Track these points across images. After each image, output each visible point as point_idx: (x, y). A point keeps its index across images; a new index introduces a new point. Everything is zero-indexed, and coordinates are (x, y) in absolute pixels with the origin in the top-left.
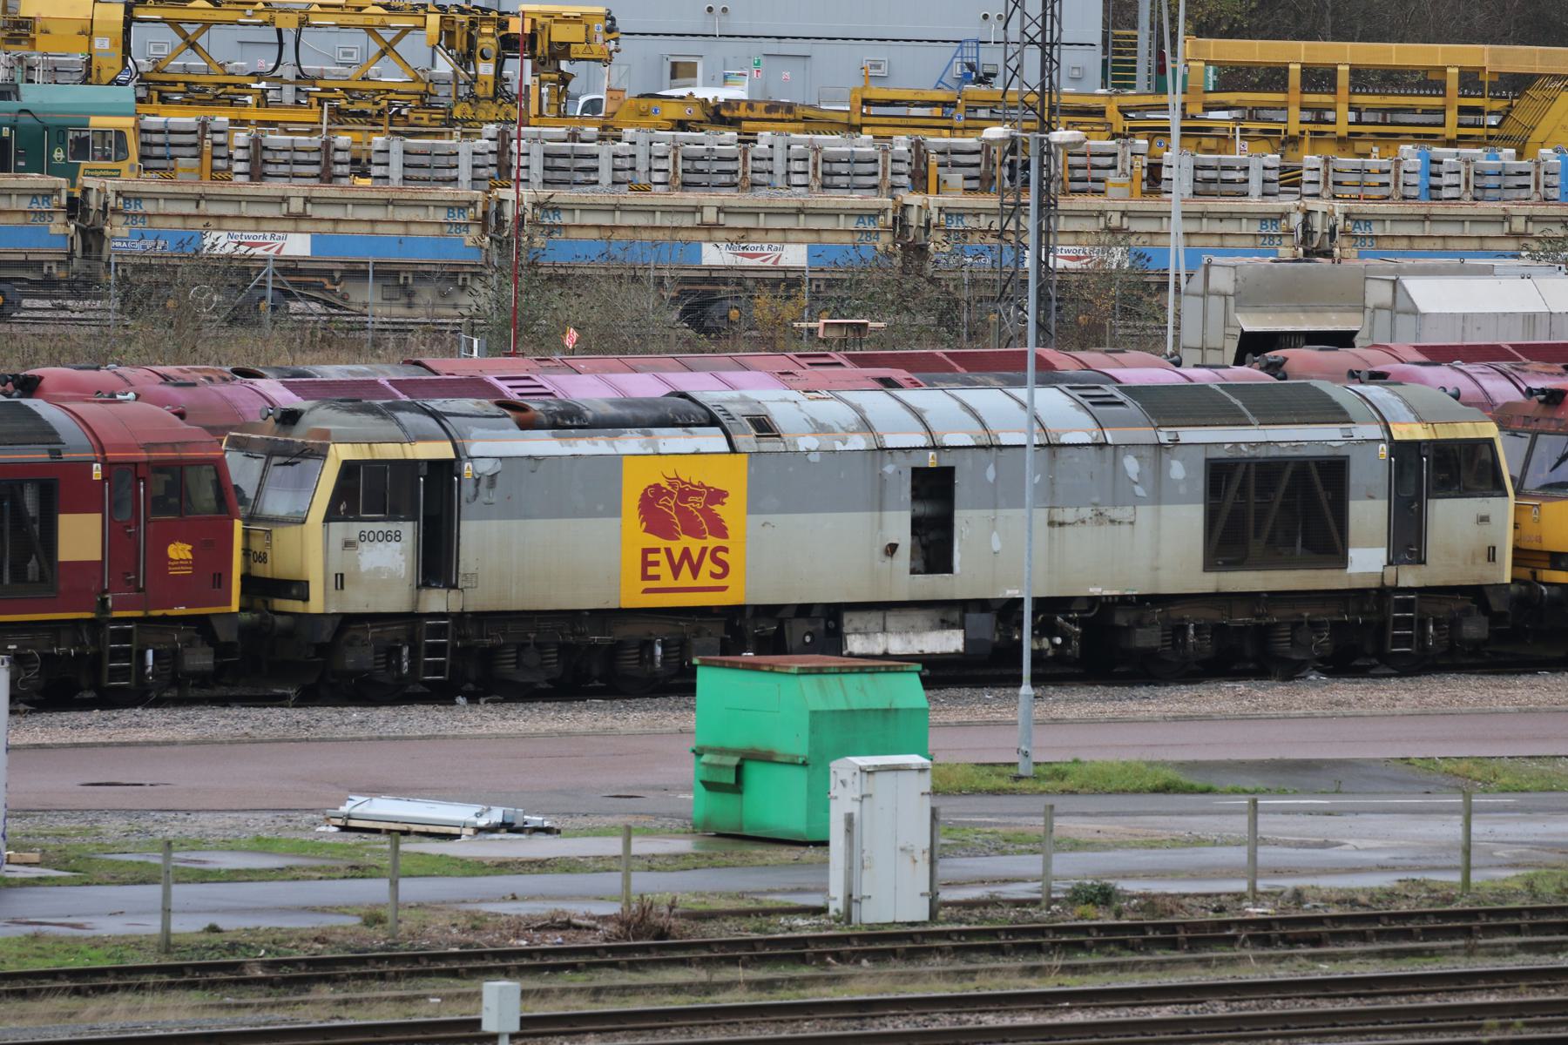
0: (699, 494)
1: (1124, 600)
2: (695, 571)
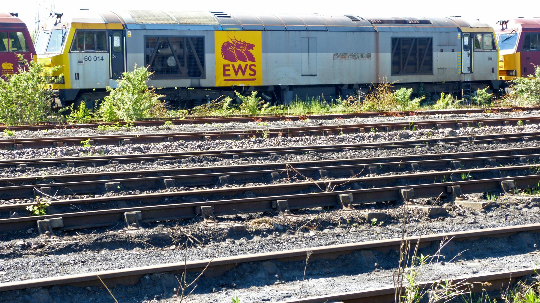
0: (244, 46)
2: (244, 73)
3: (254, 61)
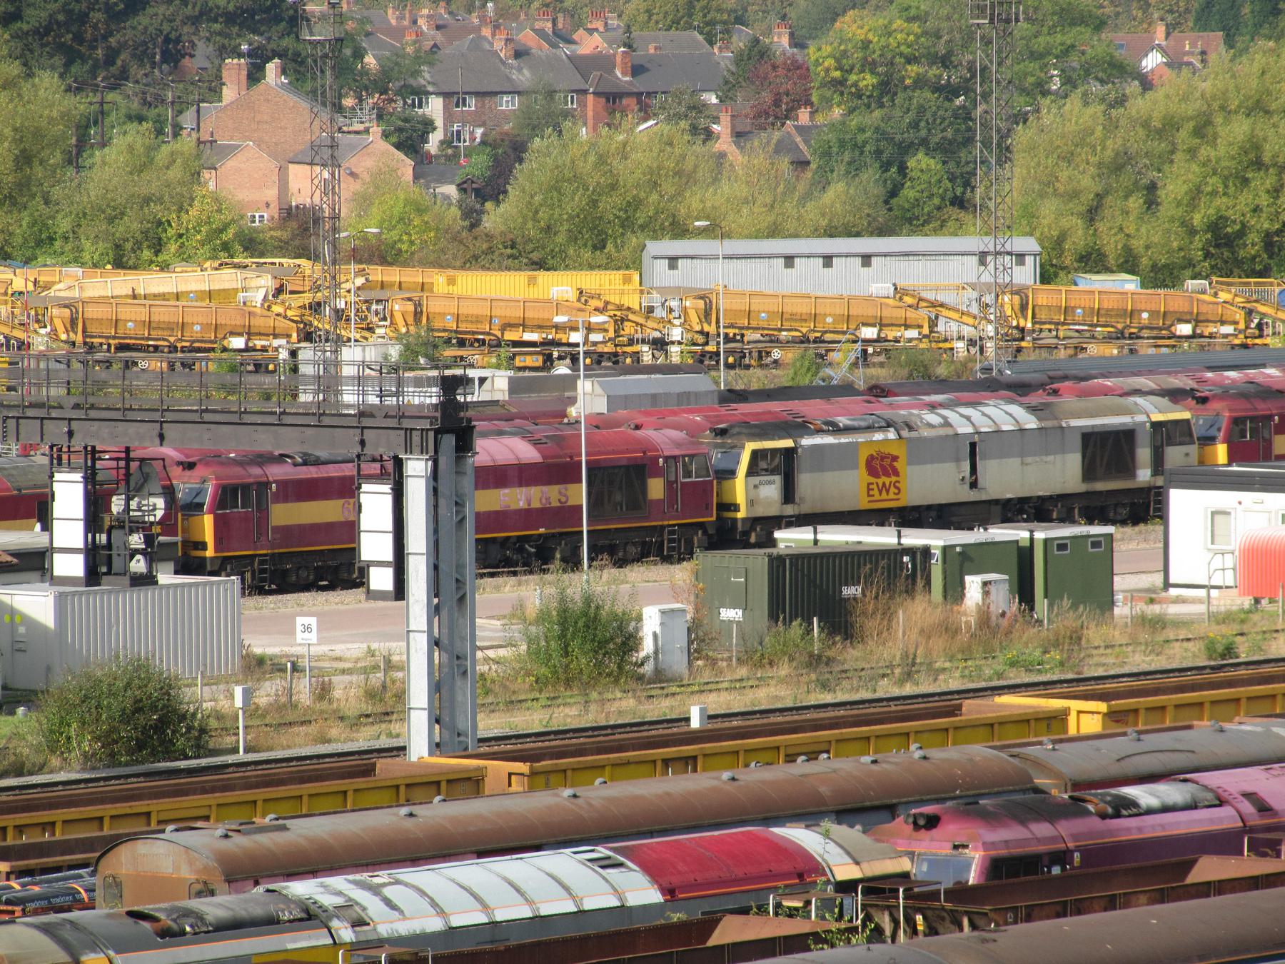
1: (1051, 497)
2: (888, 491)
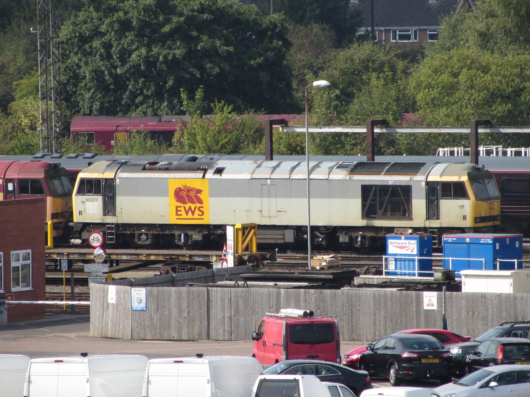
2: (193, 213)
3: (202, 204)
